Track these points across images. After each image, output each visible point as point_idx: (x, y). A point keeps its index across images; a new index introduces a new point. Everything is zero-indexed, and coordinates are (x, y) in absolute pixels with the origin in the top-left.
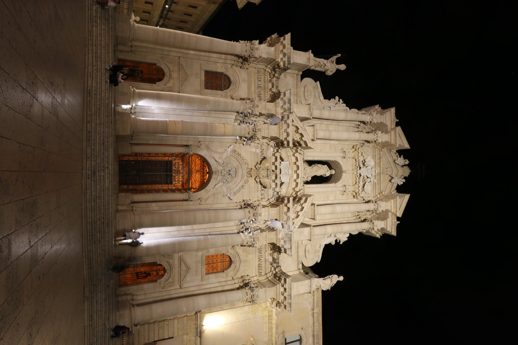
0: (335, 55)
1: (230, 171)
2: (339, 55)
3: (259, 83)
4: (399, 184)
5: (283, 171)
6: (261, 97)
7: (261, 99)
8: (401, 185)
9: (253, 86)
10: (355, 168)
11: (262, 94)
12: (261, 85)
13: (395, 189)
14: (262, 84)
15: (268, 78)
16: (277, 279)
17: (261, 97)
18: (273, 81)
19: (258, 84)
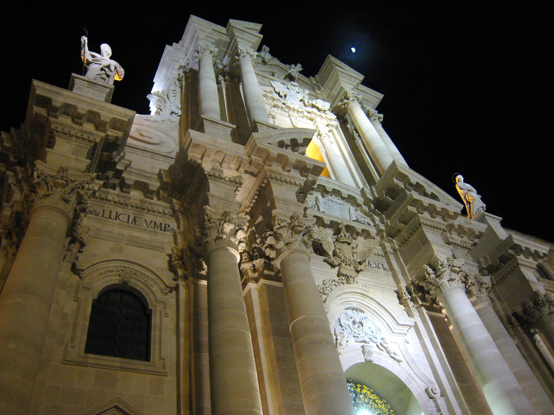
0: (79, 46)
1: (354, 323)
2: (84, 39)
3: (124, 218)
4: (300, 70)
5: (336, 213)
6: (161, 224)
7: (167, 226)
8: (302, 67)
9: (136, 234)
10: (286, 112)
11: (154, 220)
12: (129, 216)
13: (307, 79)
14: (125, 213)
15: (114, 194)
16: (503, 264)
17: (161, 224)
18: (131, 180)
19: (128, 222)
